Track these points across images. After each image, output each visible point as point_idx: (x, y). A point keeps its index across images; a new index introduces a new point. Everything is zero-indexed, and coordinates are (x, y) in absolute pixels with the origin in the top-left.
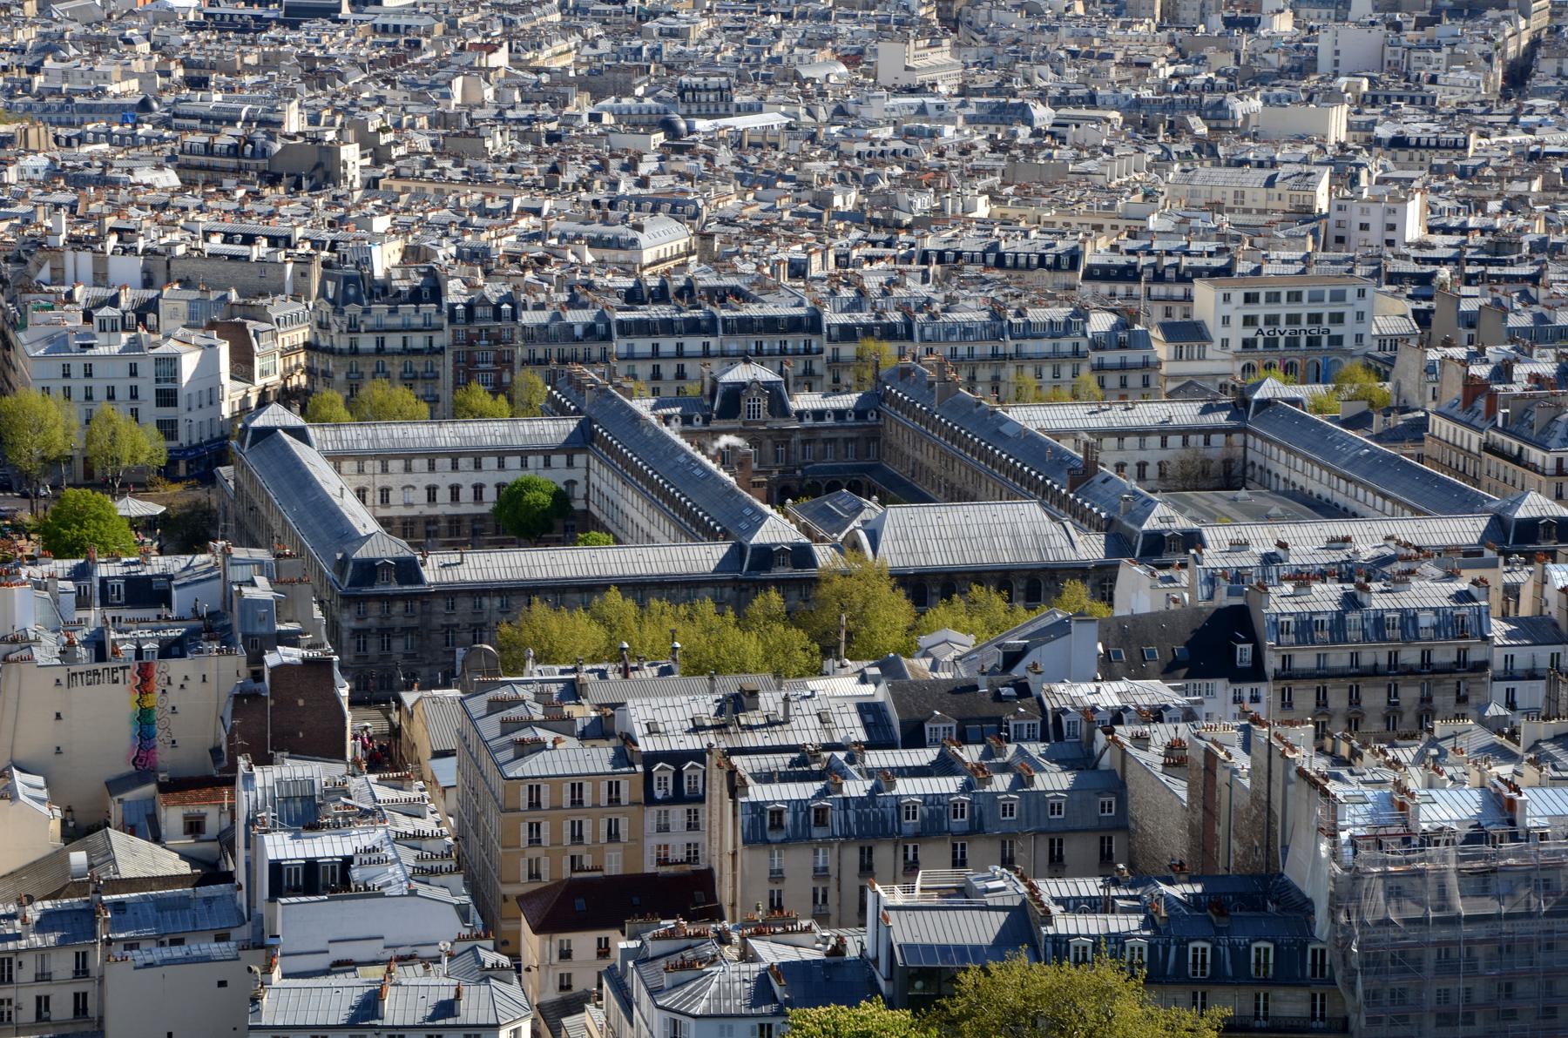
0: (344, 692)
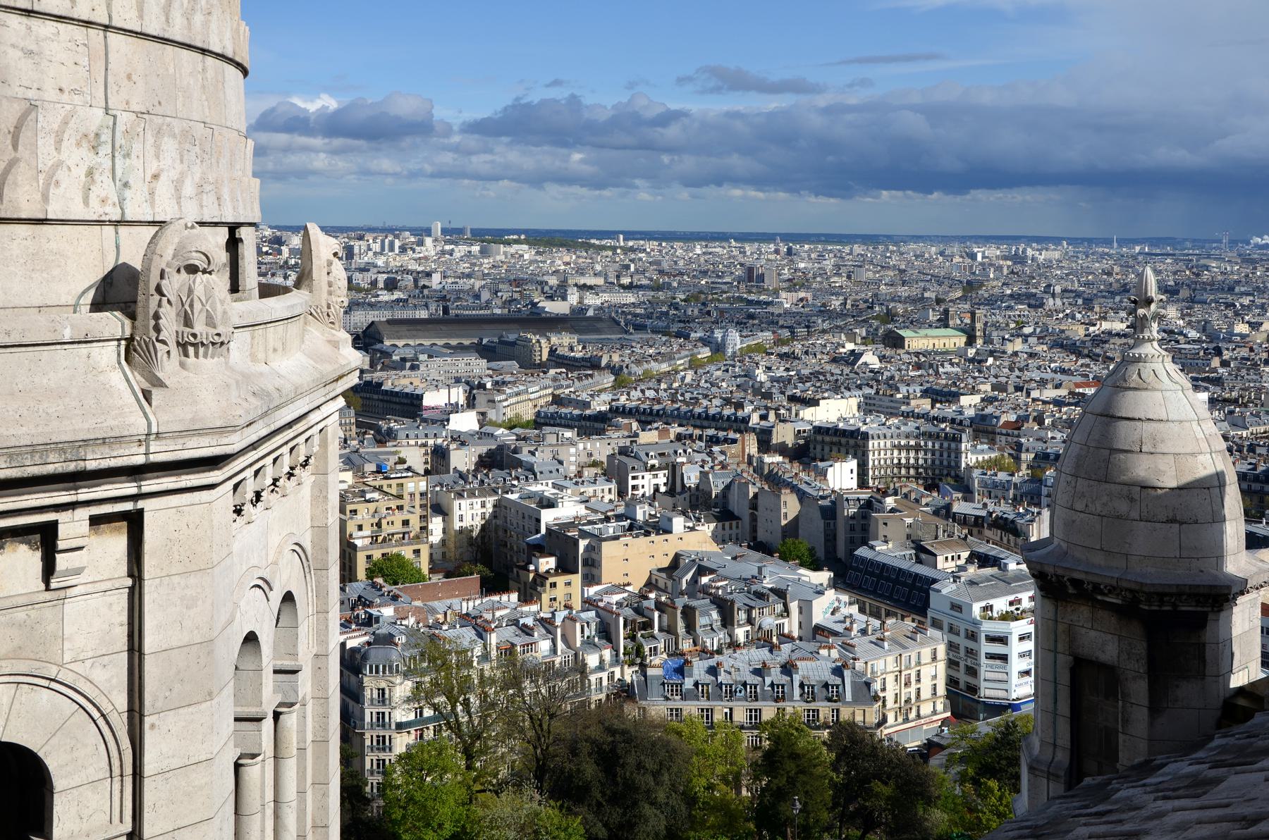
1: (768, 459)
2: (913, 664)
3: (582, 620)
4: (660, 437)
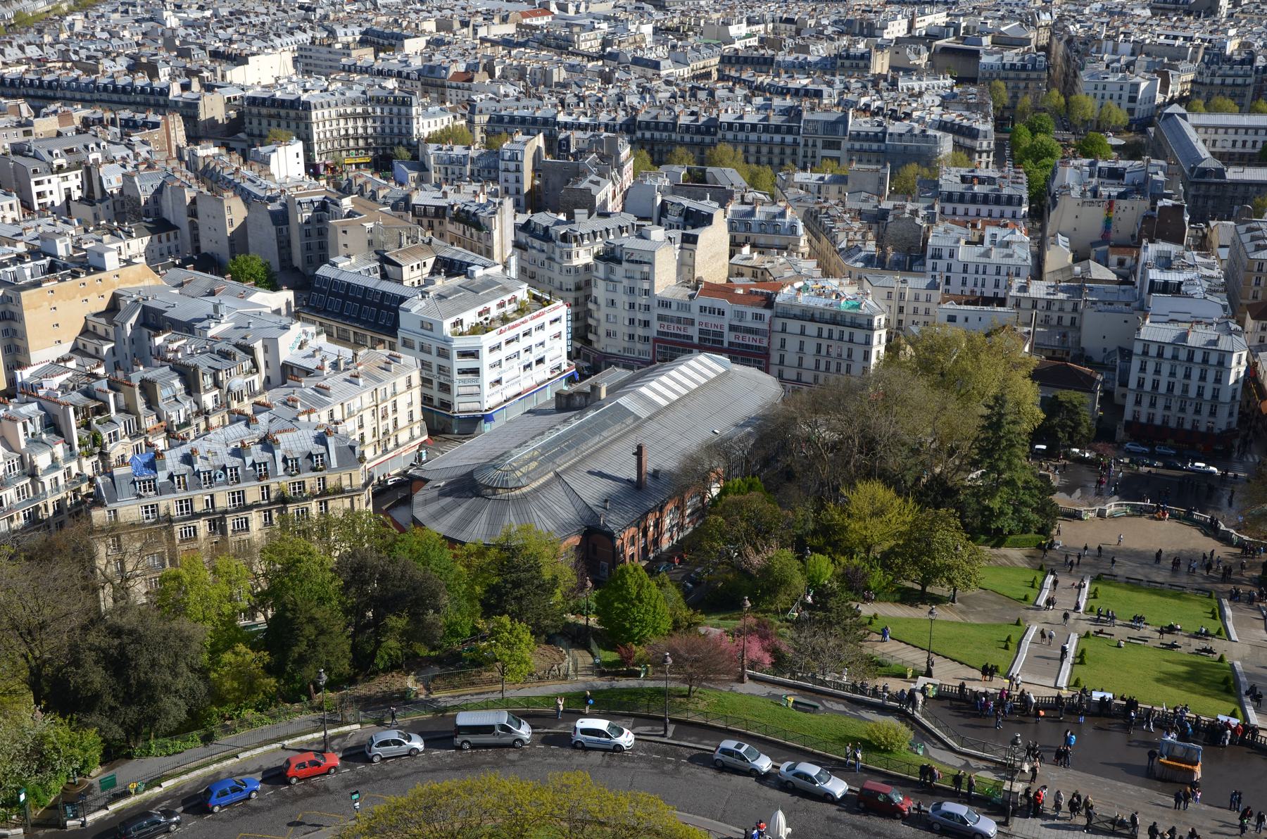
0: (1187, 219)
1: (201, 152)
2: (389, 395)
3: (23, 416)
4: (61, 123)
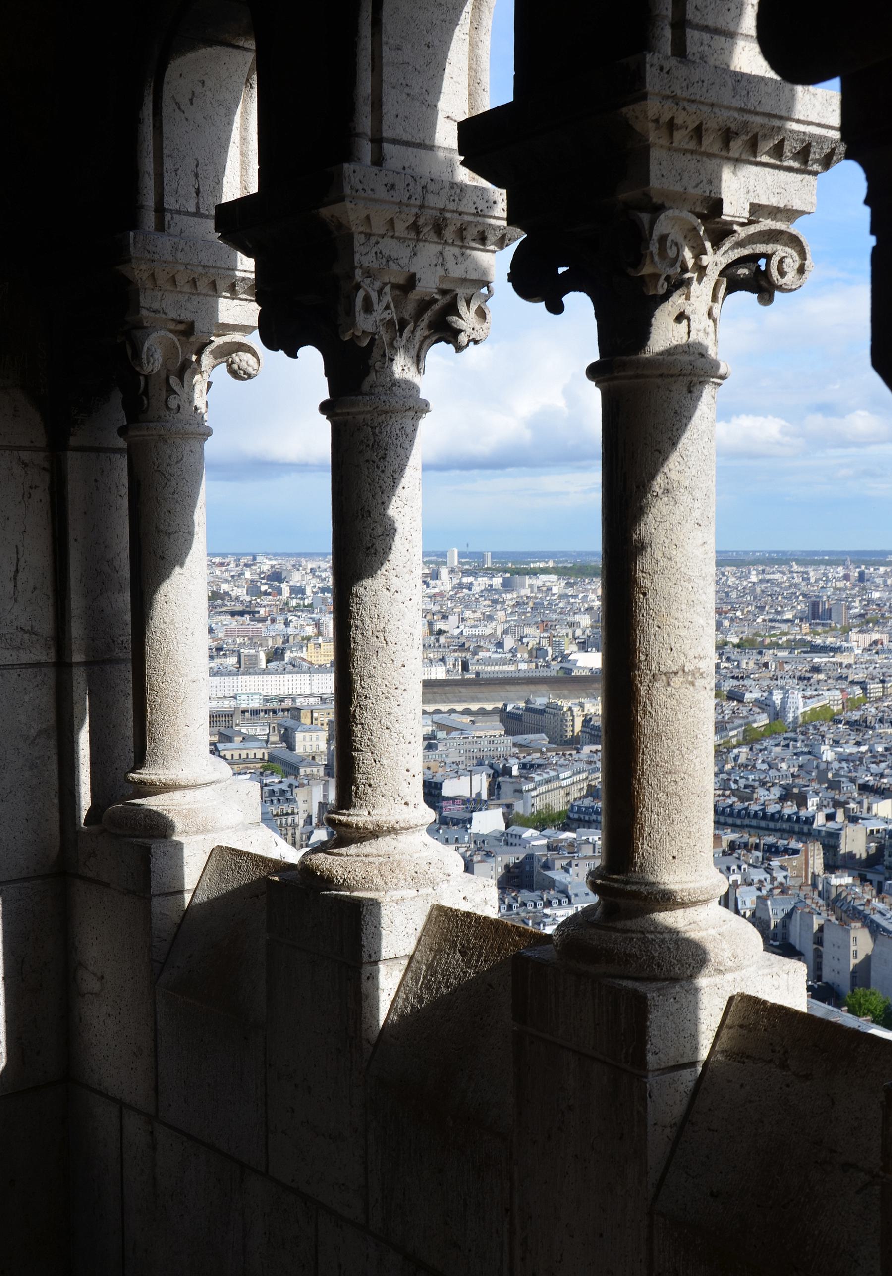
1: (835, 881)
